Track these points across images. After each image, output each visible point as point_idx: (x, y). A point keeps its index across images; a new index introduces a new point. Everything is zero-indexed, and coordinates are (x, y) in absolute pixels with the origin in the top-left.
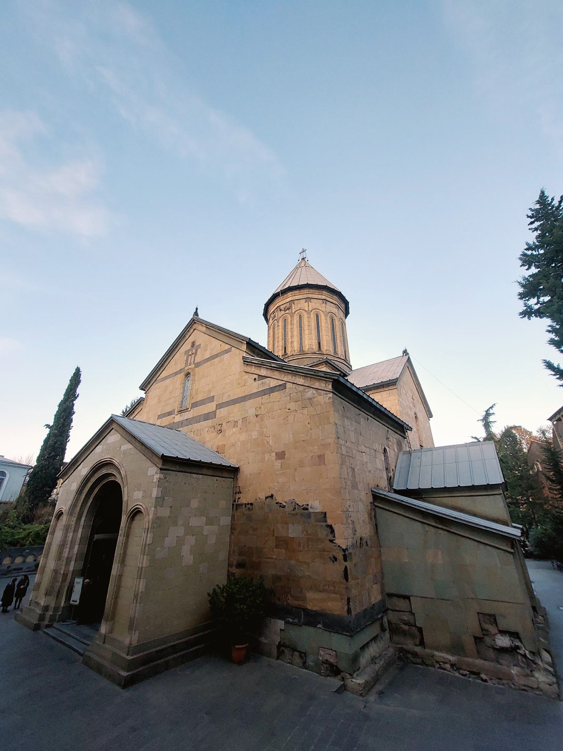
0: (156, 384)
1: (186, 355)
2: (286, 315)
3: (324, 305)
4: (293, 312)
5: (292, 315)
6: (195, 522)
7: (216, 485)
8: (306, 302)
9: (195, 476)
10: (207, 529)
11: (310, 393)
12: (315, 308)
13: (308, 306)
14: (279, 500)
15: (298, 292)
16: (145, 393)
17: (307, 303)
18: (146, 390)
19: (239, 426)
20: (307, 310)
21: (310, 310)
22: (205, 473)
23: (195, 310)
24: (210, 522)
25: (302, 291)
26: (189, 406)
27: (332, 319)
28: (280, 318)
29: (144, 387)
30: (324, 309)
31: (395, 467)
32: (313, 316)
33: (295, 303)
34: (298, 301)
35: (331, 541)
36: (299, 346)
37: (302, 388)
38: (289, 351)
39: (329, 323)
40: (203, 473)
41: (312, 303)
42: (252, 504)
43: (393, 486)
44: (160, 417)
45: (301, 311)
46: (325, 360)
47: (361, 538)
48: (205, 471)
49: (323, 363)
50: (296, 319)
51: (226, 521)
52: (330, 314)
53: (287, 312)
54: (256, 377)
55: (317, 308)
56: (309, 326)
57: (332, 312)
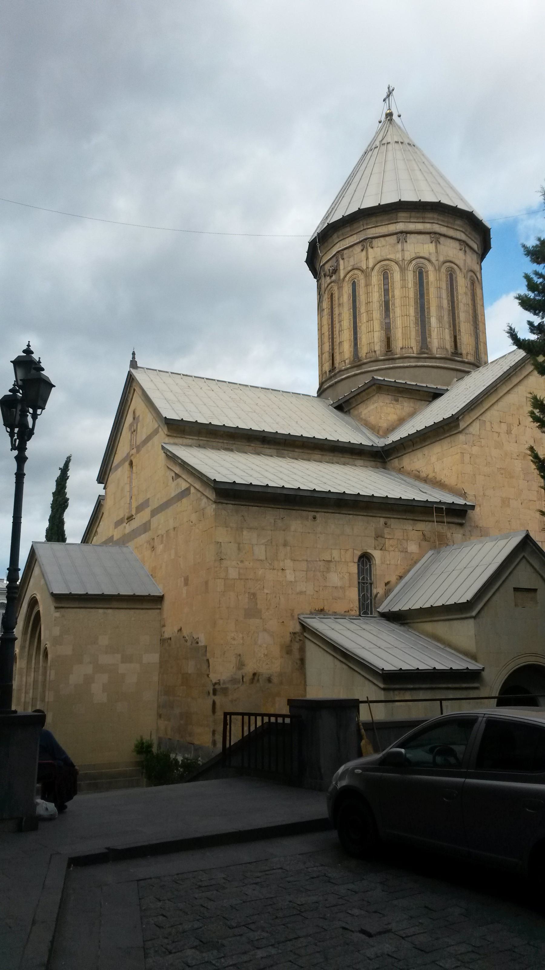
0: (111, 475)
1: (130, 432)
2: (333, 284)
3: (399, 246)
4: (342, 275)
5: (339, 283)
6: (105, 659)
7: (133, 619)
8: (362, 250)
9: (101, 611)
10: (123, 668)
11: (205, 500)
12: (380, 258)
13: (367, 259)
14: (185, 635)
15: (348, 229)
16: (105, 488)
17: (364, 253)
18: (105, 483)
19: (164, 542)
20: (365, 268)
21: (371, 265)
22: (116, 606)
23: (131, 356)
24: (127, 659)
25: (355, 225)
26: (133, 512)
27: (421, 273)
28: (325, 293)
29: (102, 478)
30: (399, 256)
31: (401, 577)
32: (376, 279)
33: (345, 256)
34: (351, 249)
35: (208, 675)
36: (352, 349)
37: (199, 495)
38: (337, 365)
39: (410, 284)
40: (112, 606)
41: (375, 249)
42: (170, 639)
43: (379, 607)
44: (118, 523)
45: (356, 272)
46: (372, 383)
47: (254, 674)
48: (115, 604)
49: (374, 387)
50: (347, 289)
51: (153, 658)
52: (414, 262)
53: (334, 278)
54: (173, 475)
55: (385, 257)
56: (368, 303)
57: (422, 255)
